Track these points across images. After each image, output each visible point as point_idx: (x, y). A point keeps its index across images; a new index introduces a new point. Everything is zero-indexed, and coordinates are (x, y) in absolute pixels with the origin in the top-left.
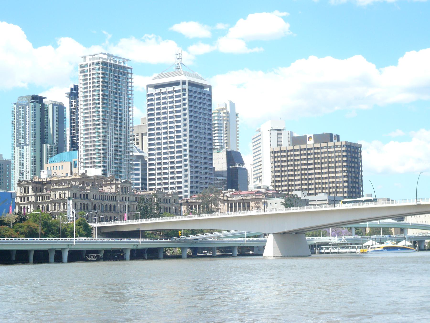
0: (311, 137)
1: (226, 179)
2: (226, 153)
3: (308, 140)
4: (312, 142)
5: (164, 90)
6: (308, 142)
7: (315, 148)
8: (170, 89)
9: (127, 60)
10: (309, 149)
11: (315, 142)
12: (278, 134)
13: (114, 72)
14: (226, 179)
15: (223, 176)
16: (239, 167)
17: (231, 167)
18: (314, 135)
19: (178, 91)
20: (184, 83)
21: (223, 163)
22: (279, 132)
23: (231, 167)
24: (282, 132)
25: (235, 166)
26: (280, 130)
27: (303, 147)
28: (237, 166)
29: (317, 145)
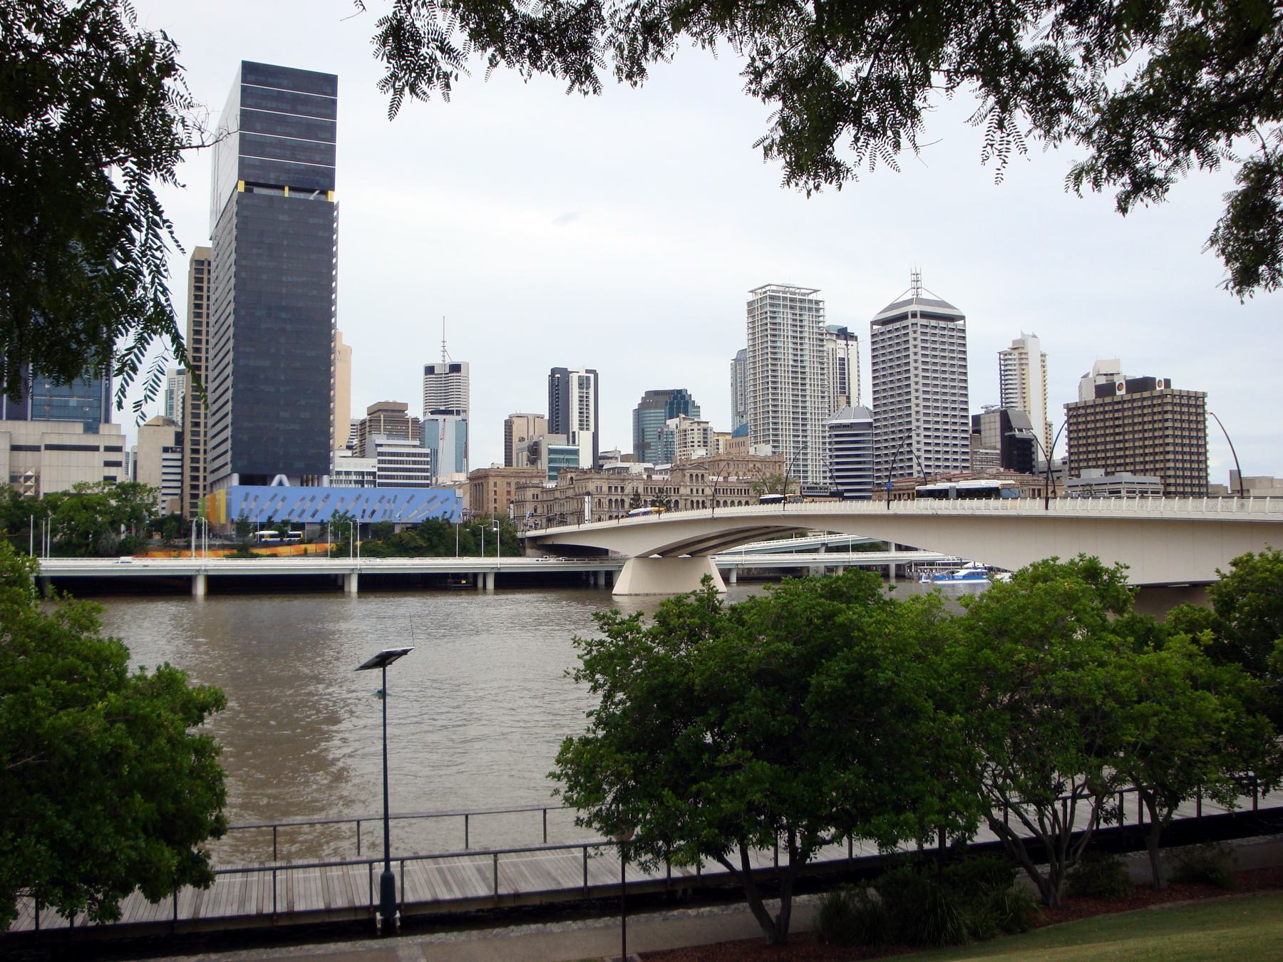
1: (998, 452)
4: (1123, 392)
5: (890, 327)
6: (1118, 393)
7: (1125, 402)
8: (897, 325)
9: (816, 291)
10: (1118, 403)
11: (1127, 392)
13: (792, 308)
14: (998, 452)
15: (995, 448)
19: (907, 327)
20: (914, 315)
23: (1007, 434)
26: (1112, 374)
29: (1128, 397)
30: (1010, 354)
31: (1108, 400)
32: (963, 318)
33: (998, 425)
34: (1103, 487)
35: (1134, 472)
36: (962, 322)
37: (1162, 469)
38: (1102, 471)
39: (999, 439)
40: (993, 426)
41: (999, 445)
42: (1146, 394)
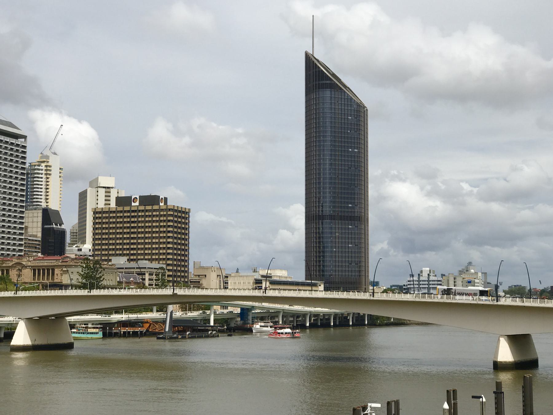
0: (136, 198)
1: (40, 239)
2: (41, 211)
3: (134, 202)
4: (137, 204)
6: (133, 204)
7: (139, 211)
10: (133, 211)
11: (140, 204)
12: (106, 192)
14: (40, 239)
16: (57, 227)
17: (46, 226)
18: (140, 197)
21: (37, 222)
22: (108, 190)
23: (46, 226)
24: (112, 190)
25: (52, 226)
27: (127, 208)
28: (54, 226)
29: (142, 208)
30: (39, 166)
31: (127, 208)
32: (25, 137)
33: (40, 219)
34: (132, 270)
35: (151, 260)
36: (23, 140)
37: (164, 259)
38: (125, 258)
39: (40, 230)
40: (35, 219)
41: (40, 235)
42: (156, 207)
